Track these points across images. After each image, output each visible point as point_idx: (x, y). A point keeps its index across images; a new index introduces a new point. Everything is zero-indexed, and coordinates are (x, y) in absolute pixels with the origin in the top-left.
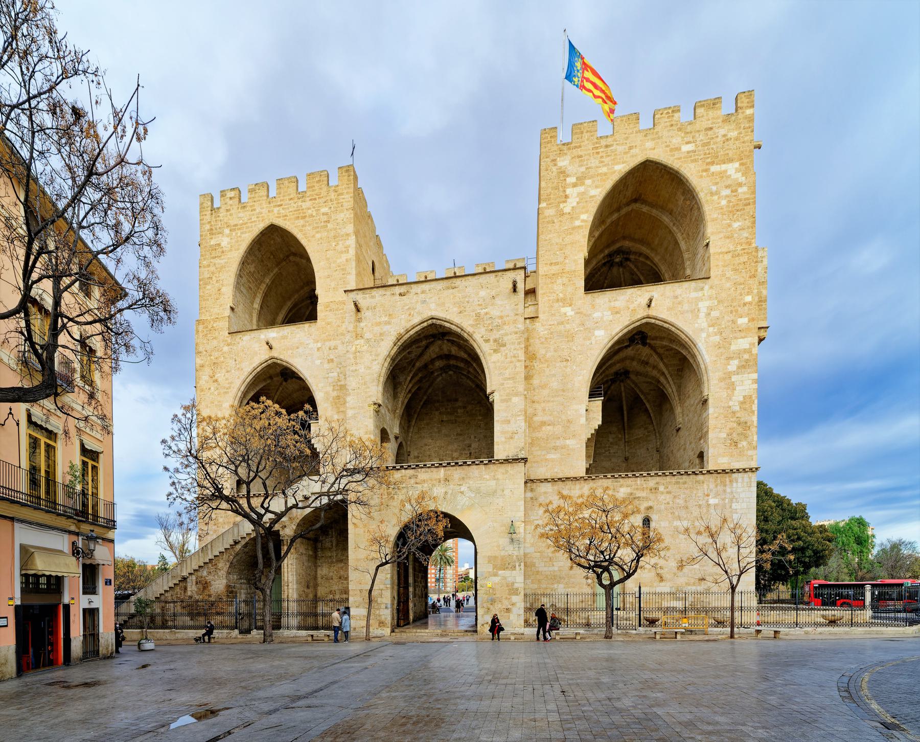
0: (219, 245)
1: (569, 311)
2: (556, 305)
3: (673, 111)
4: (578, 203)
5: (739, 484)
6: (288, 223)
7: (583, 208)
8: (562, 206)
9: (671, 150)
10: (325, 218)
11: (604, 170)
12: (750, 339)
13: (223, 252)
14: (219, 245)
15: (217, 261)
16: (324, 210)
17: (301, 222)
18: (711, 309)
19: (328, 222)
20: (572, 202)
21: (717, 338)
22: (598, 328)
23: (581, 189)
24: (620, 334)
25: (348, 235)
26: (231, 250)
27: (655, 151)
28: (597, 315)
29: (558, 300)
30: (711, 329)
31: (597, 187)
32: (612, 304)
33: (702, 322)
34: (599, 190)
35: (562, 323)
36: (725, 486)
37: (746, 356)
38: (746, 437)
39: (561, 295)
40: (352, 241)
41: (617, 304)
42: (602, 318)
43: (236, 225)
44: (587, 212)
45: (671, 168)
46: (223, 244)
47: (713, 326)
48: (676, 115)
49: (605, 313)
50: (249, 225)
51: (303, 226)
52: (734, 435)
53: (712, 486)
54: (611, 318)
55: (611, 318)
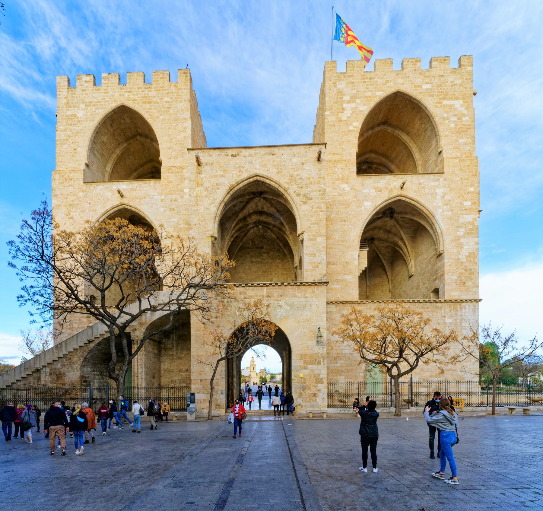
0: (75, 115)
1: (346, 187)
2: (337, 182)
3: (416, 61)
4: (351, 114)
5: (467, 310)
6: (137, 106)
8: (340, 115)
9: (415, 86)
10: (167, 105)
11: (369, 94)
12: (473, 215)
13: (78, 121)
14: (75, 115)
15: (73, 127)
16: (167, 99)
17: (148, 106)
18: (444, 194)
20: (348, 113)
21: (450, 213)
23: (354, 105)
24: (381, 206)
25: (185, 119)
26: (86, 121)
28: (365, 191)
29: (338, 179)
30: (445, 207)
31: (364, 105)
32: (376, 185)
33: (439, 202)
34: (366, 107)
35: (342, 195)
36: (457, 311)
37: (470, 227)
38: (471, 279)
39: (340, 176)
41: (379, 185)
42: (369, 194)
43: (90, 102)
44: (357, 121)
45: (414, 99)
46: (78, 115)
47: (446, 205)
48: (418, 64)
51: (149, 109)
52: (463, 277)
53: (447, 310)
54: (375, 194)
55: (375, 194)
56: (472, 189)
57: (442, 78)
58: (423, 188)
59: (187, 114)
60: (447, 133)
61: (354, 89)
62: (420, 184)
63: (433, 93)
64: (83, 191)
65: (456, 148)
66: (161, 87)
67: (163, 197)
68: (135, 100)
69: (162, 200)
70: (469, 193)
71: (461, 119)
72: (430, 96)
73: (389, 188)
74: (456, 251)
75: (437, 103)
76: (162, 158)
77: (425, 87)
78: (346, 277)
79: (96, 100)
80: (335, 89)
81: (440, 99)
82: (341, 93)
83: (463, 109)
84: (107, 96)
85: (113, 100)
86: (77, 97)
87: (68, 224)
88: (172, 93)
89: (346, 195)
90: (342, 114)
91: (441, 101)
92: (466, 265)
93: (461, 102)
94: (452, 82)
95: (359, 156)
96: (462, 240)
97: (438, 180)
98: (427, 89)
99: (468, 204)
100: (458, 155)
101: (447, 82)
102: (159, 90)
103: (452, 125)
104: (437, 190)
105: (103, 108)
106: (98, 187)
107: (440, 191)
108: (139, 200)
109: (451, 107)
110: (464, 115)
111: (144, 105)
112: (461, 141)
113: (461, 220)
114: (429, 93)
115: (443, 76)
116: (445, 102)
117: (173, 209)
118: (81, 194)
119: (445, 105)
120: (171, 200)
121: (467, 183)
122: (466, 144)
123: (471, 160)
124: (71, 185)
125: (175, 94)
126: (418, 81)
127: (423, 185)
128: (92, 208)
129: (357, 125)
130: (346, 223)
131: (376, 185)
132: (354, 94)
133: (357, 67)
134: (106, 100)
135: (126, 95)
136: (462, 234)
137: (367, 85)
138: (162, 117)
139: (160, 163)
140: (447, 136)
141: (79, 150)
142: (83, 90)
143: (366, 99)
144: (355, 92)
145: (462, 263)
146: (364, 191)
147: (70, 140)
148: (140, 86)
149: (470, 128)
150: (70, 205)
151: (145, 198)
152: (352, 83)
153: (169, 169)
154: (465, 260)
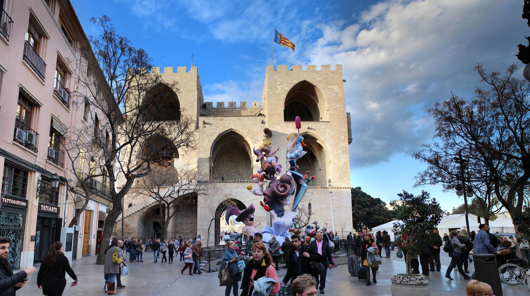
11: (290, 81)
16: (185, 81)
20: (279, 90)
21: (333, 142)
23: (282, 87)
25: (194, 91)
37: (344, 149)
56: (344, 130)
59: (195, 88)
77: (318, 79)
83: (338, 90)
95: (285, 111)
96: (340, 156)
103: (333, 98)
107: (327, 131)
109: (332, 89)
110: (339, 93)
112: (338, 106)
116: (329, 87)
126: (315, 76)
129: (284, 96)
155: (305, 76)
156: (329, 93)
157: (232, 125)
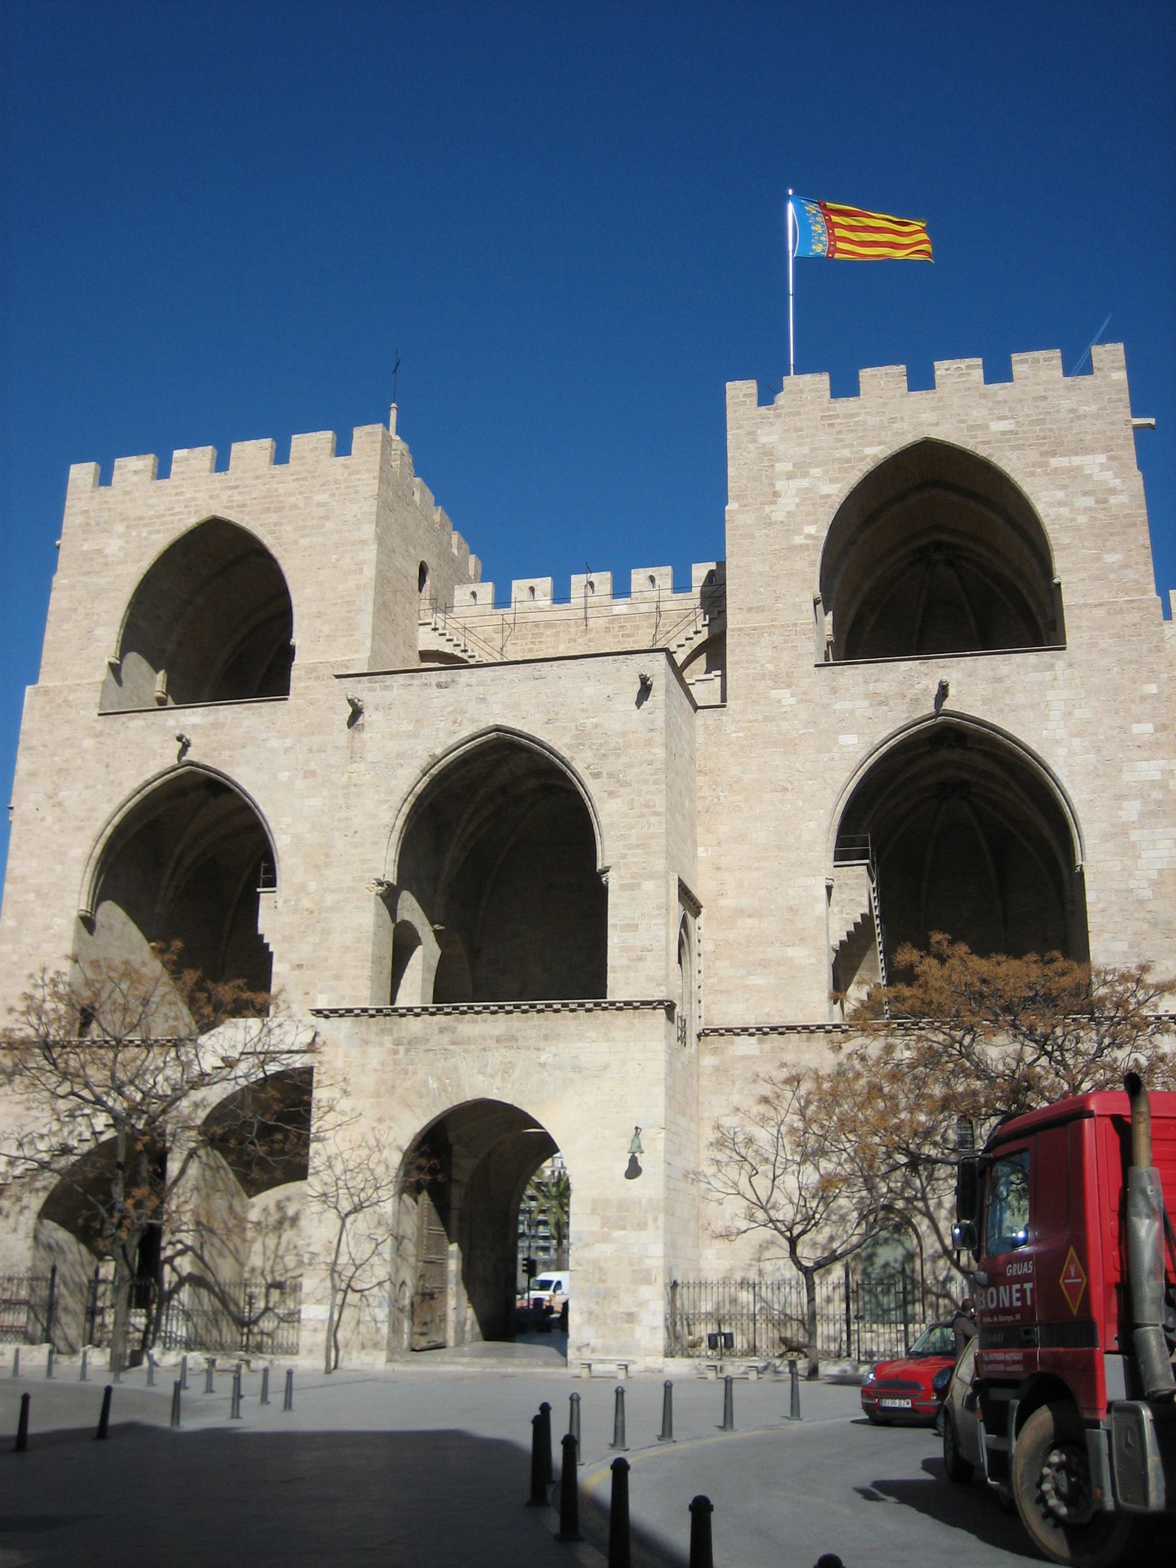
0: (99, 551)
1: (786, 697)
4: (797, 505)
7: (808, 514)
8: (767, 509)
9: (971, 428)
11: (846, 453)
12: (1162, 762)
13: (106, 564)
16: (322, 497)
17: (273, 517)
19: (327, 518)
21: (1092, 757)
22: (847, 732)
23: (805, 483)
25: (363, 542)
27: (939, 428)
29: (763, 677)
30: (1076, 742)
31: (832, 481)
32: (871, 687)
37: (1157, 795)
39: (770, 667)
40: (371, 553)
41: (882, 687)
42: (852, 712)
43: (140, 518)
44: (815, 522)
46: (108, 551)
47: (1078, 735)
49: (858, 703)
50: (168, 519)
51: (276, 524)
54: (869, 712)
56: (1152, 689)
57: (1042, 404)
58: (1006, 691)
60: (1068, 541)
61: (800, 445)
62: (999, 680)
63: (1021, 442)
64: (96, 736)
65: (1098, 578)
66: (309, 472)
67: (289, 742)
68: (244, 505)
69: (287, 750)
70: (1143, 699)
71: (1105, 501)
72: (1013, 448)
73: (910, 693)
74: (1119, 868)
75: (1034, 465)
76: (296, 640)
77: (997, 426)
78: (790, 952)
79: (152, 513)
80: (752, 447)
81: (1043, 454)
82: (768, 454)
84: (179, 501)
85: (192, 509)
86: (109, 510)
87: (49, 819)
88: (336, 482)
89: (785, 719)
90: (773, 507)
91: (1044, 459)
92: (1151, 906)
93: (1102, 458)
94: (1071, 411)
96: (1134, 836)
97: (1051, 667)
98: (1003, 433)
99: (1144, 729)
100: (1106, 597)
101: (1058, 411)
102: (304, 479)
103: (1082, 519)
104: (1050, 695)
105: (167, 530)
106: (132, 724)
108: (228, 753)
109: (1075, 473)
110: (1113, 491)
111: (264, 516)
112: (1109, 558)
113: (1127, 777)
114: (1009, 440)
115: (1044, 398)
116: (1055, 462)
117: (313, 774)
118: (89, 743)
119: (1056, 469)
120: (310, 751)
121: (1137, 671)
122: (1128, 566)
123: (1140, 609)
124: (69, 722)
125: (343, 485)
126: (977, 414)
127: (1007, 684)
128: (111, 777)
129: (817, 531)
130: (789, 796)
131: (871, 687)
132: (805, 456)
133: (811, 391)
134: (176, 510)
135: (225, 496)
136: (1135, 818)
137: (840, 432)
138: (304, 542)
139: (288, 653)
140: (1068, 546)
141: (99, 631)
142: (126, 493)
143: (837, 466)
144: (805, 450)
145: (1141, 902)
146: (838, 706)
147: (81, 610)
148: (259, 473)
149: (1134, 525)
150: (60, 770)
151: (244, 747)
152: (801, 430)
153: (312, 670)
154: (1147, 893)
155: (928, 417)
156: (1060, 495)
157: (497, 709)
